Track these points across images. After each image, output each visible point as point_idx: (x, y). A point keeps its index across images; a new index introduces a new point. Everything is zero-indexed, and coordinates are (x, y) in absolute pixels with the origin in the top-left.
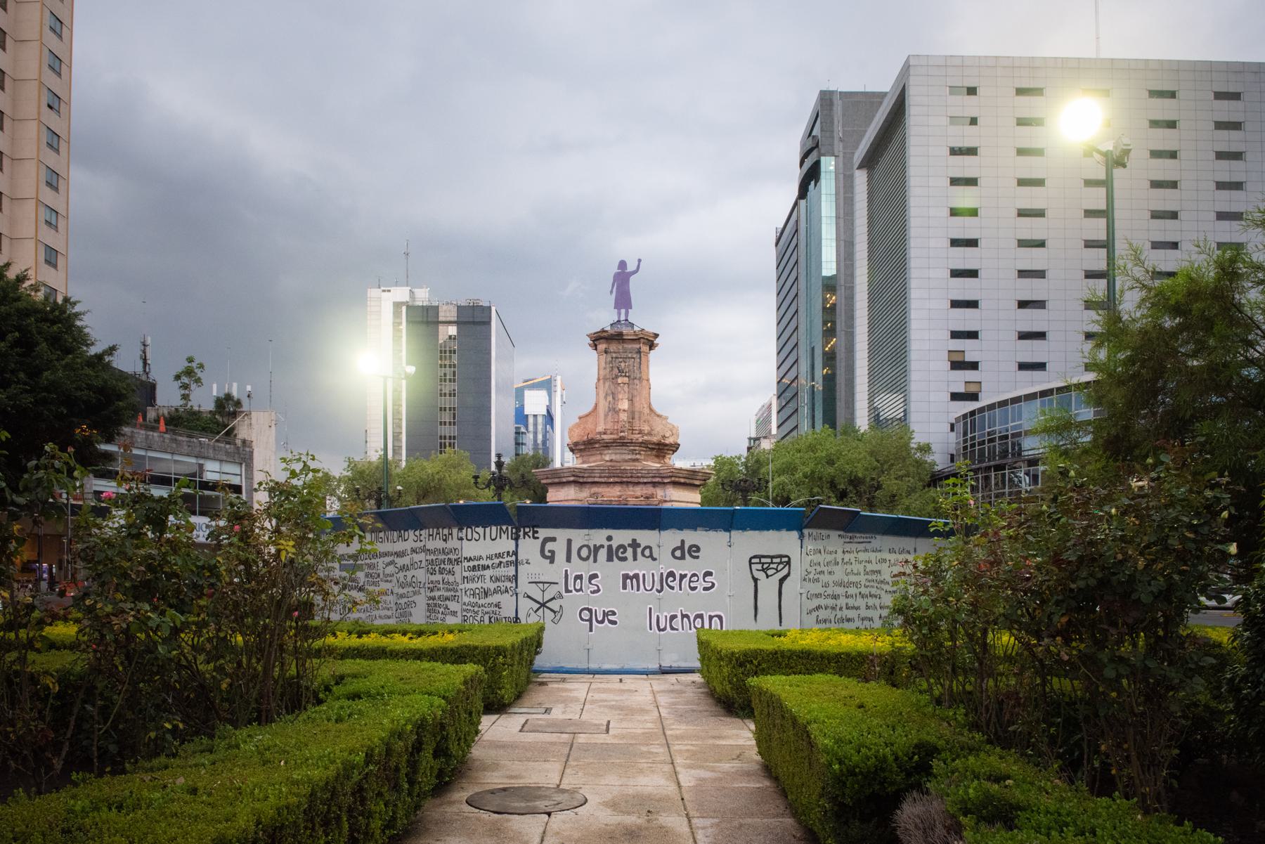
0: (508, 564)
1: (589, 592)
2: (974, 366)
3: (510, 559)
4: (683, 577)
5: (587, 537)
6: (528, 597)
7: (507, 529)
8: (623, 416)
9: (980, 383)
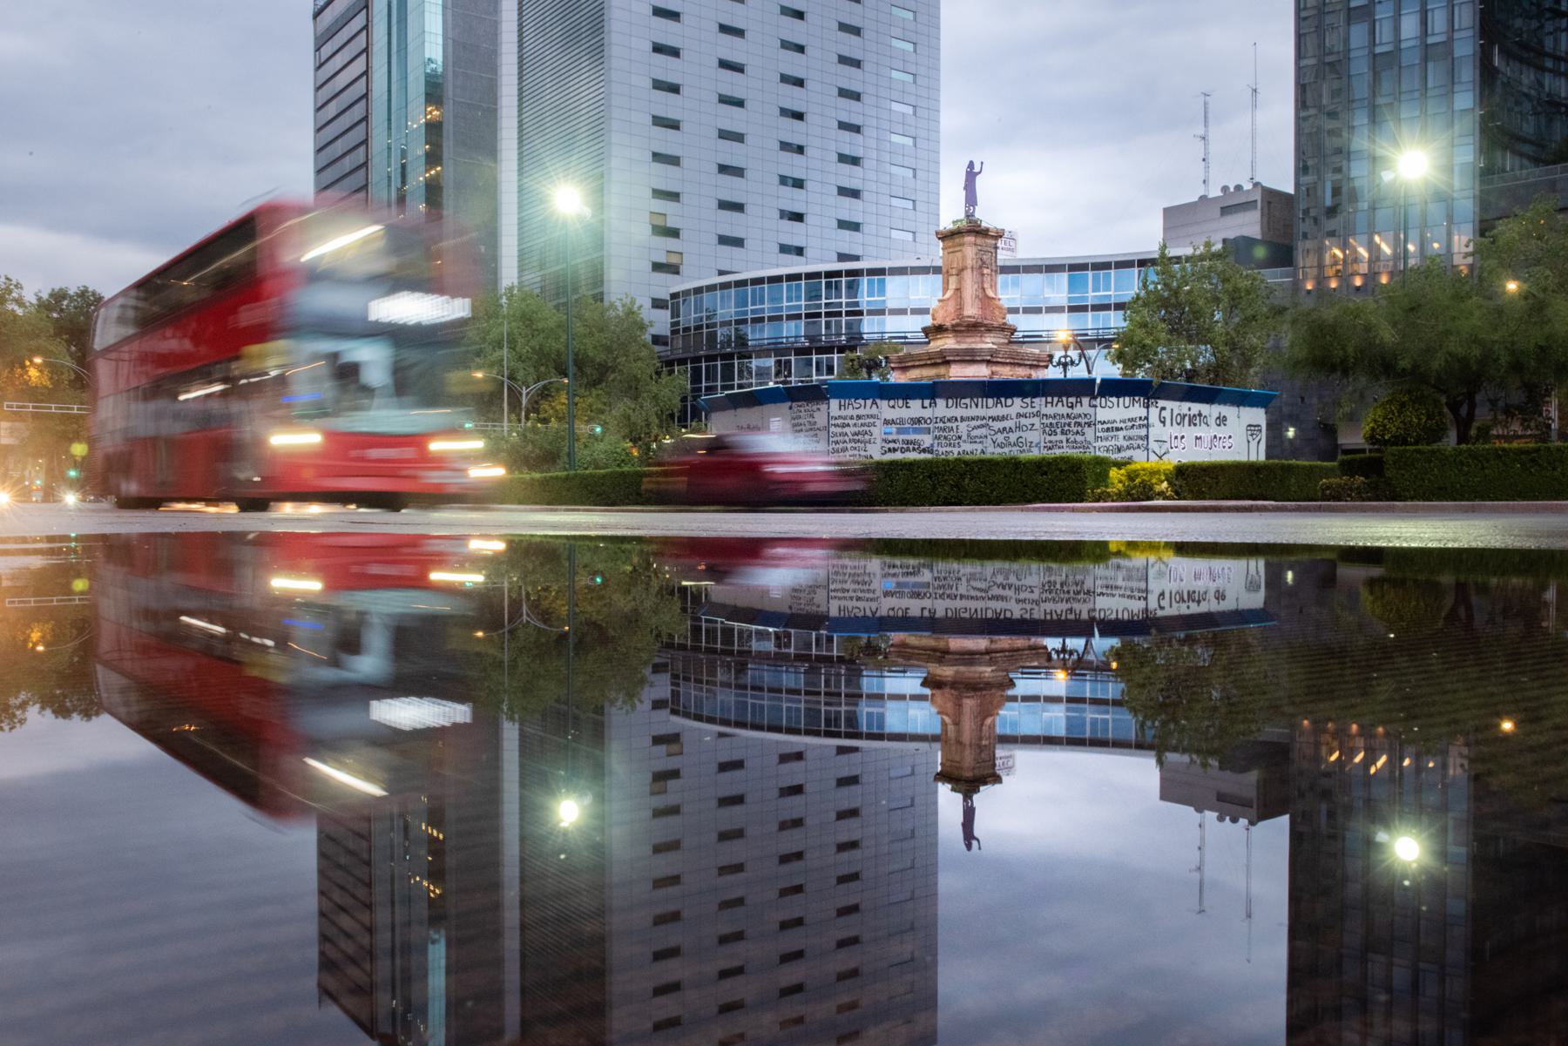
0: (1140, 426)
3: (1141, 422)
9: (681, 254)
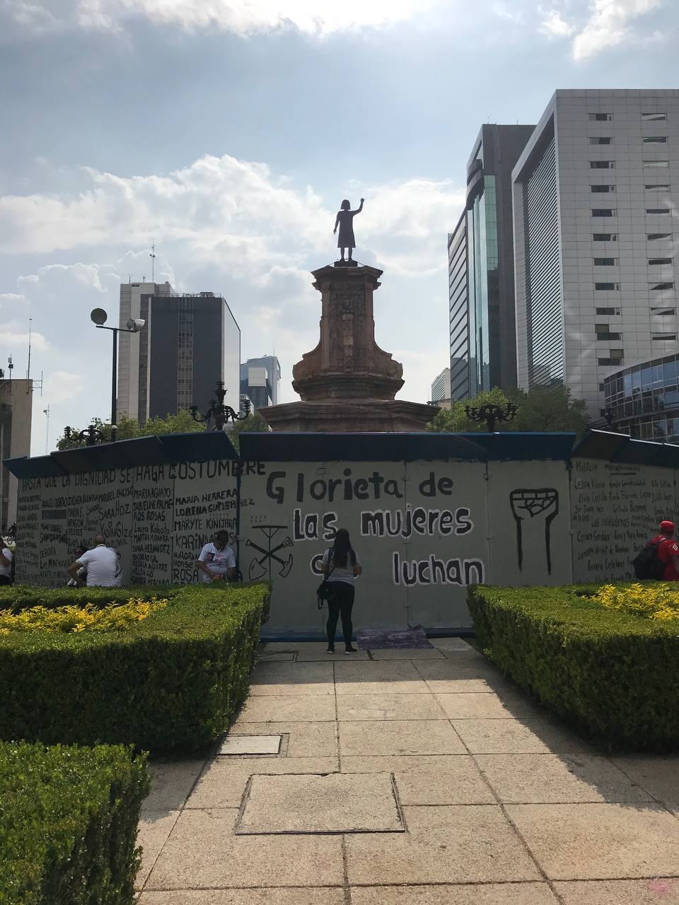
0: (228, 505)
1: (324, 538)
2: (616, 336)
3: (230, 499)
4: (433, 516)
5: (321, 471)
6: (252, 545)
7: (228, 463)
8: (349, 352)
